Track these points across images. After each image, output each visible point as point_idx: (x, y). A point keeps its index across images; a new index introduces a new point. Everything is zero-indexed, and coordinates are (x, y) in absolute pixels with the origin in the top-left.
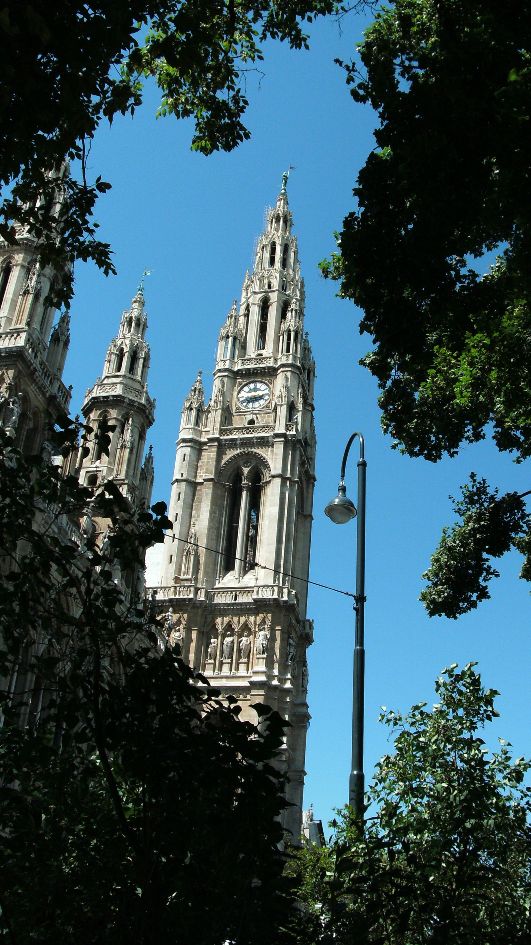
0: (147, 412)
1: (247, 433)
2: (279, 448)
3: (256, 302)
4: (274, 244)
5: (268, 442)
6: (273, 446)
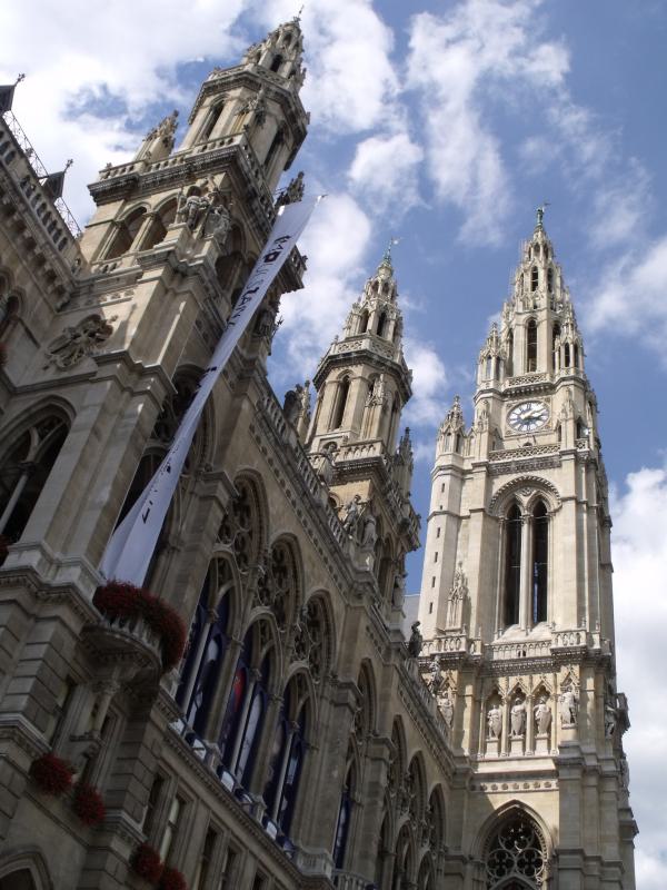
0: (403, 377)
5: (552, 463)
6: (560, 466)
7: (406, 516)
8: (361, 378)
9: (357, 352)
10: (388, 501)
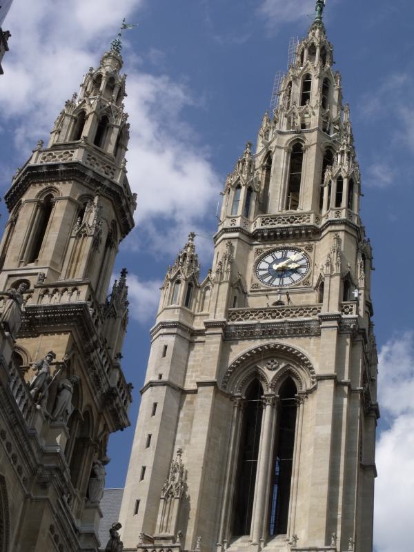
0: (124, 202)
1: (274, 318)
2: (329, 337)
3: (283, 145)
6: (318, 335)
7: (114, 384)
8: (70, 199)
9: (65, 165)
10: (91, 363)
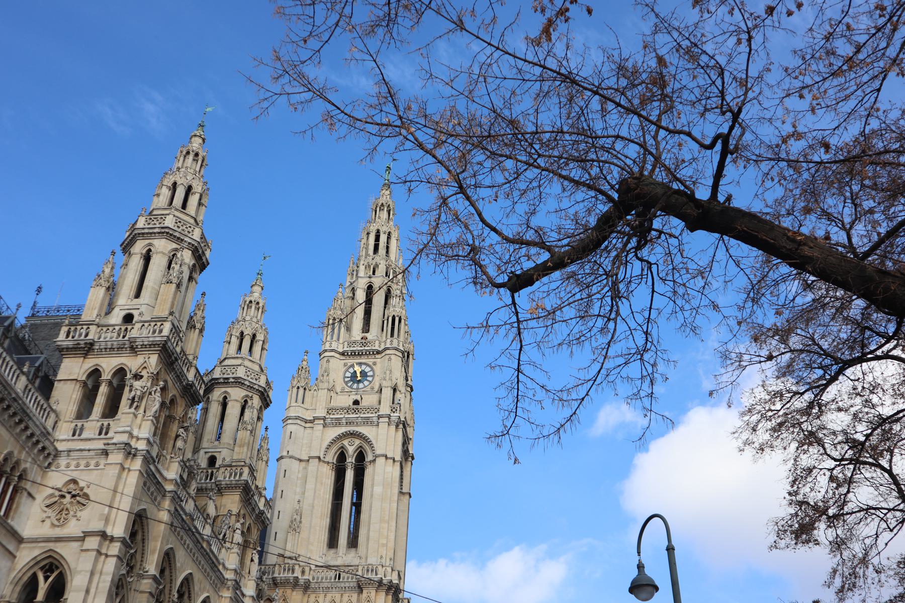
4: (378, 231)
